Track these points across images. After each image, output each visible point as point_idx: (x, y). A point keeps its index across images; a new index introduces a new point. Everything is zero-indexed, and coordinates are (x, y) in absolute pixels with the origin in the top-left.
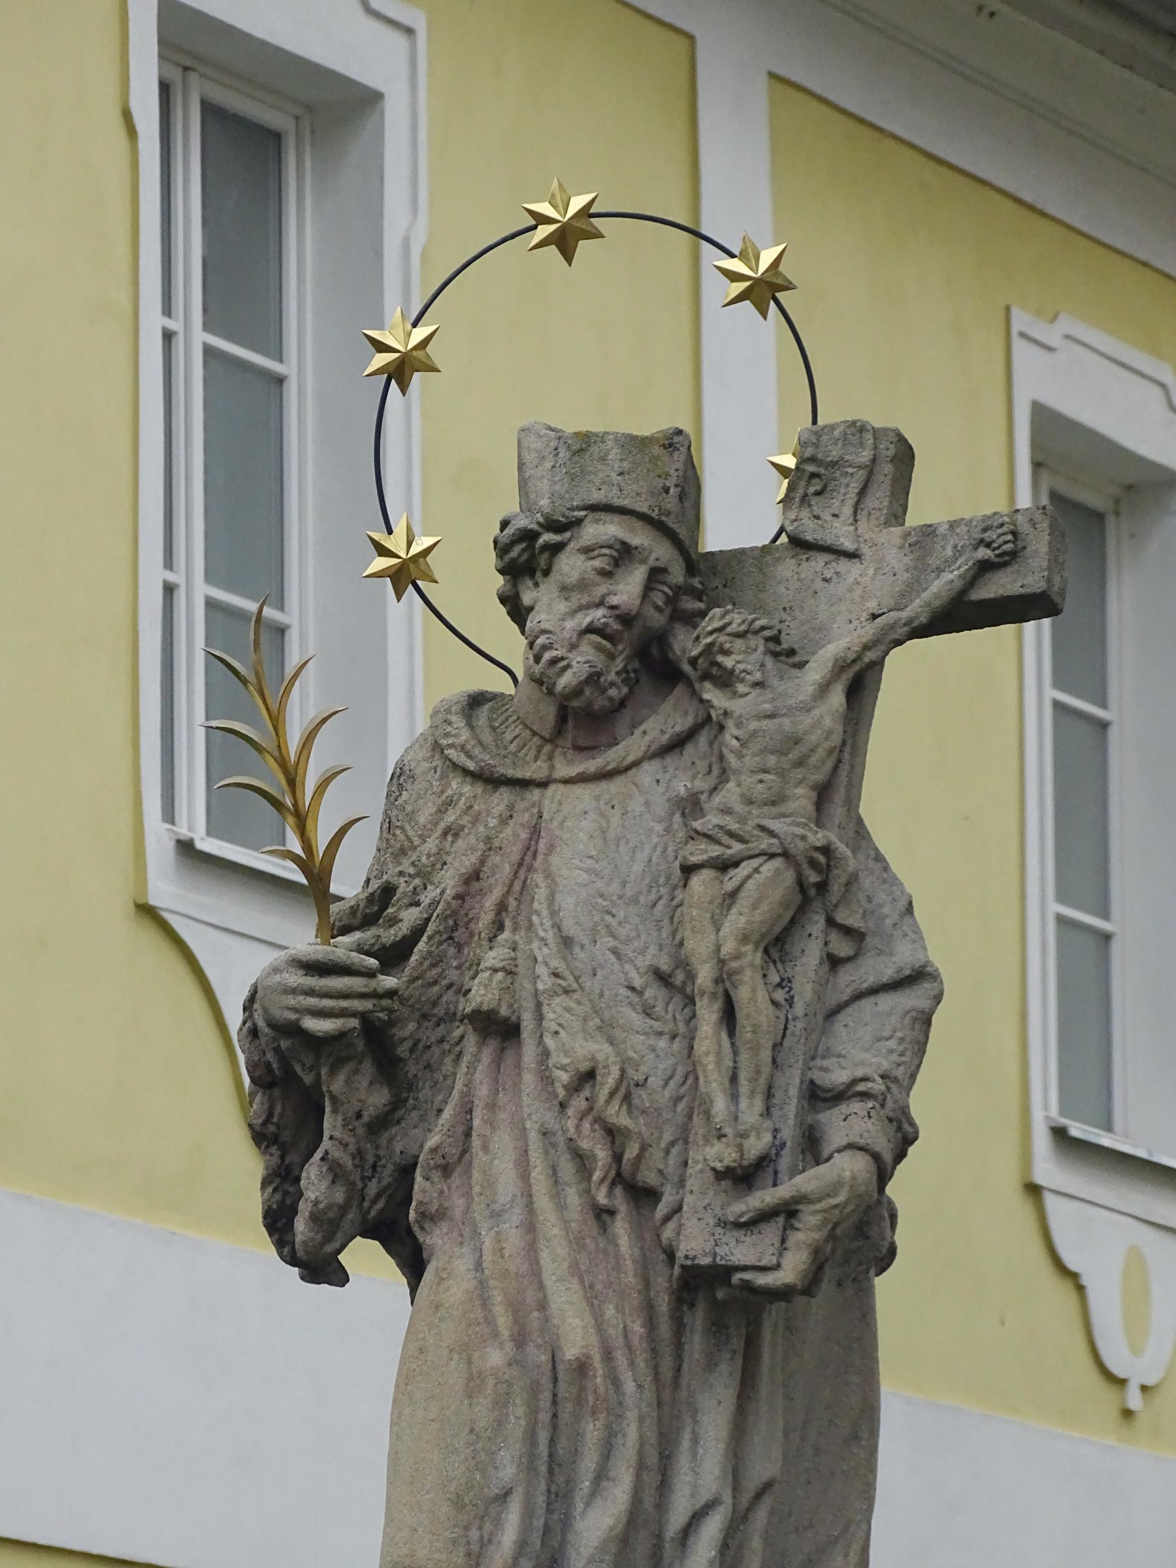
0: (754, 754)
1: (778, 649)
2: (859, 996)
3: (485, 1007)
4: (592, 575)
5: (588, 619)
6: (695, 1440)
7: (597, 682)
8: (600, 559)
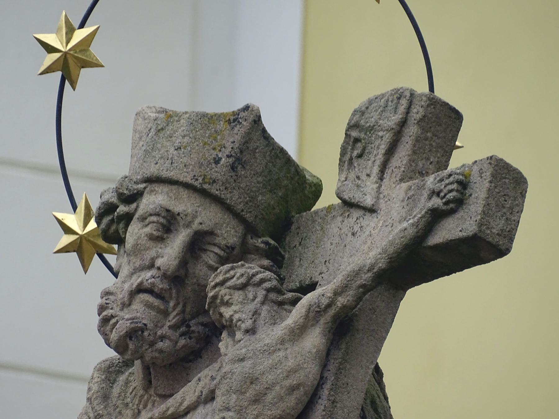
0: (223, 395)
1: (280, 298)
4: (144, 241)
5: (139, 280)
7: (142, 335)
8: (150, 226)
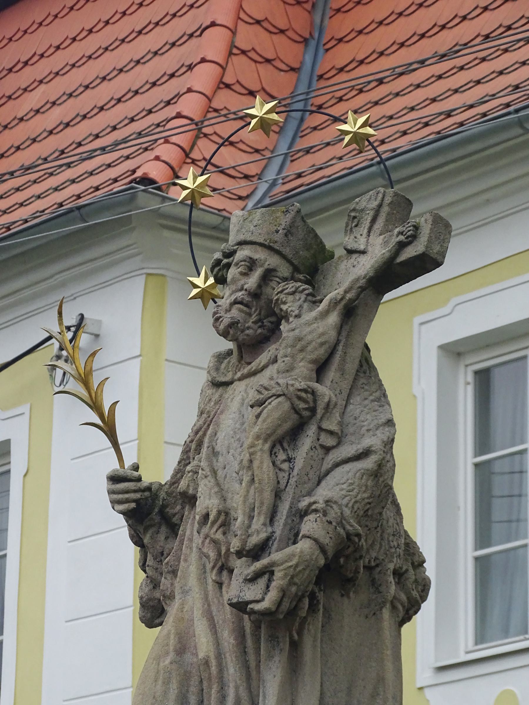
1: (314, 299)
2: (337, 465)
4: (238, 276)
5: (235, 297)
7: (237, 326)
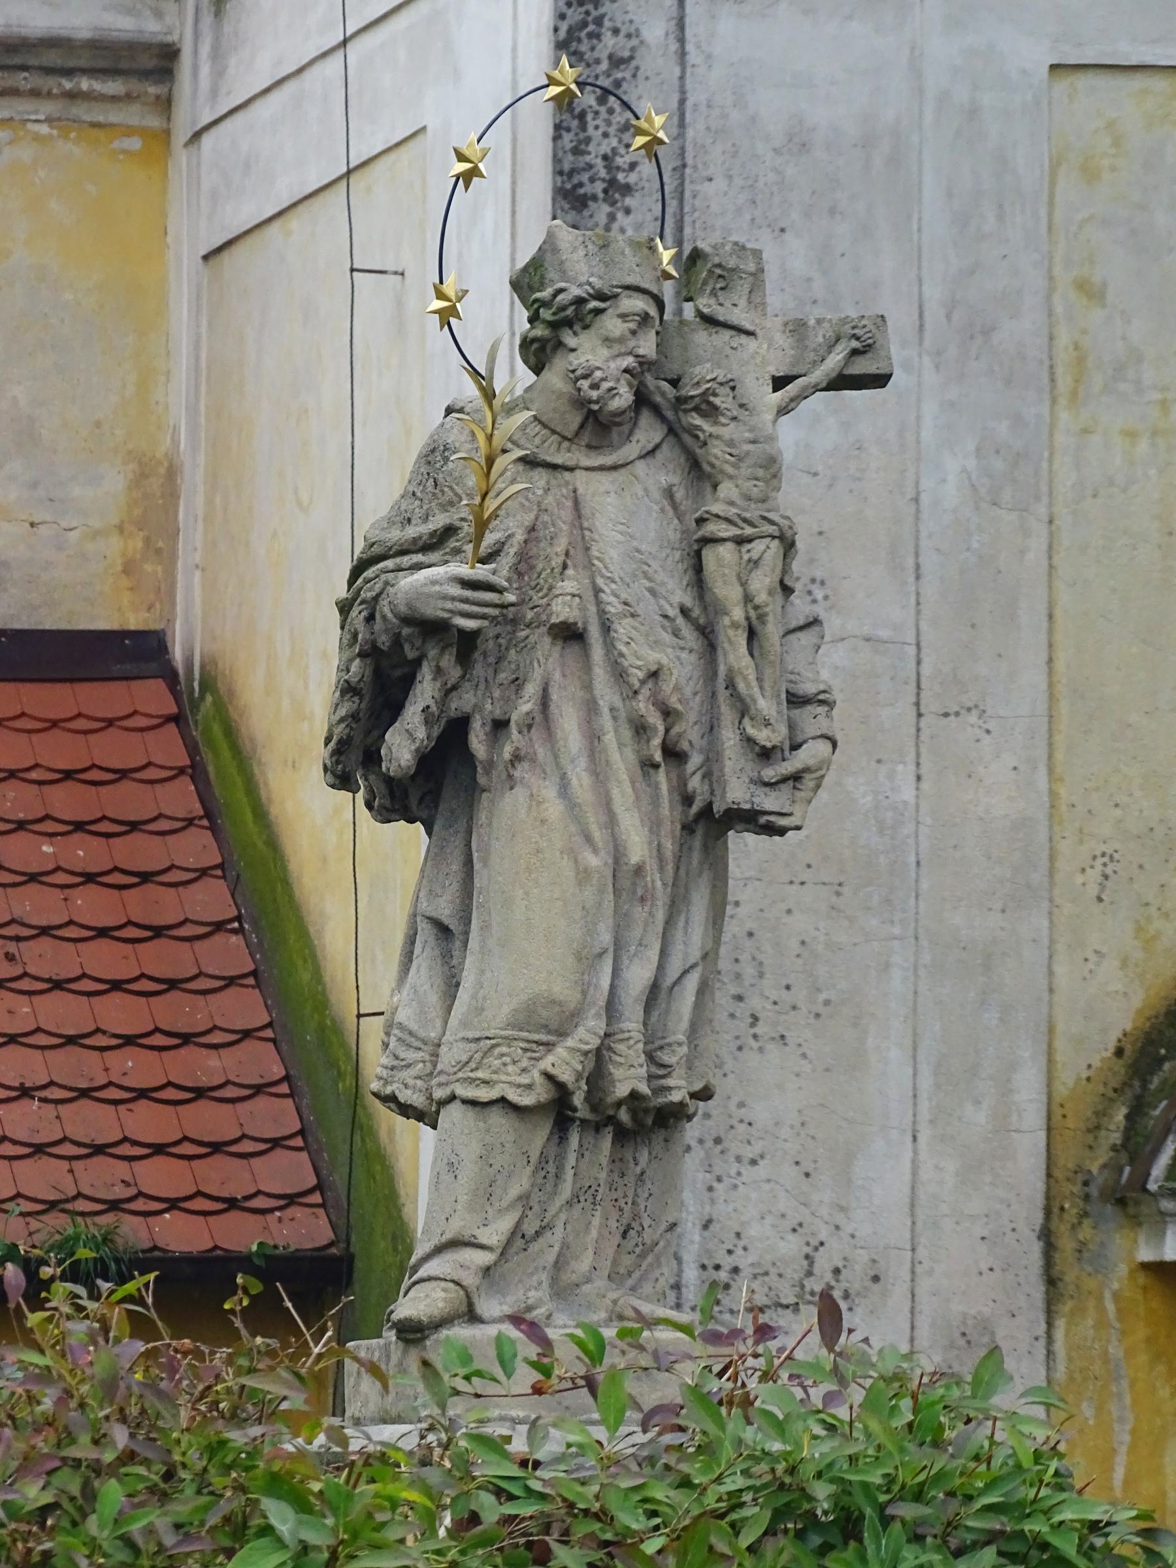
3: (571, 620)
6: (687, 922)
